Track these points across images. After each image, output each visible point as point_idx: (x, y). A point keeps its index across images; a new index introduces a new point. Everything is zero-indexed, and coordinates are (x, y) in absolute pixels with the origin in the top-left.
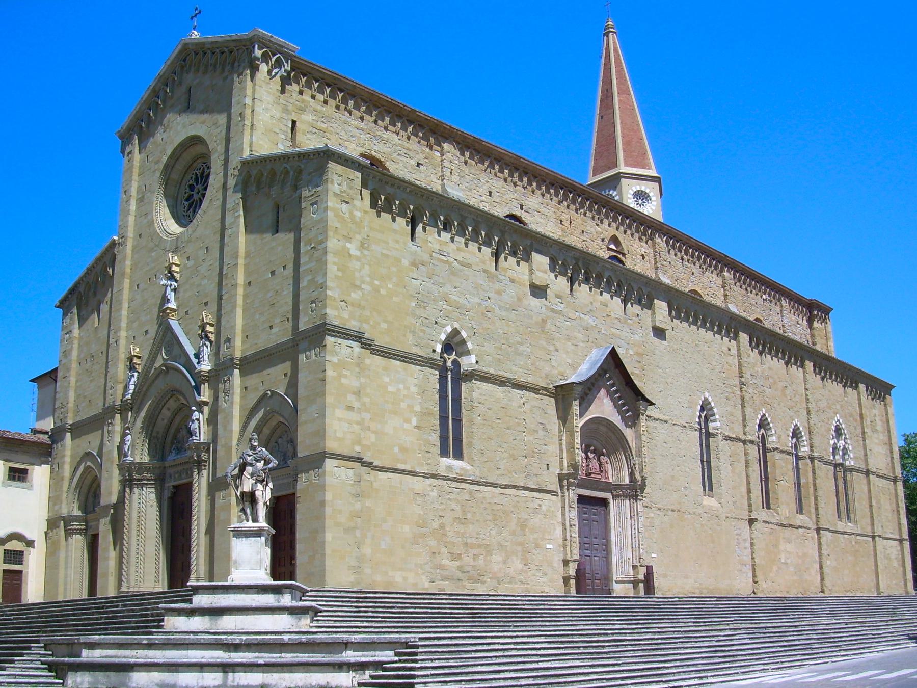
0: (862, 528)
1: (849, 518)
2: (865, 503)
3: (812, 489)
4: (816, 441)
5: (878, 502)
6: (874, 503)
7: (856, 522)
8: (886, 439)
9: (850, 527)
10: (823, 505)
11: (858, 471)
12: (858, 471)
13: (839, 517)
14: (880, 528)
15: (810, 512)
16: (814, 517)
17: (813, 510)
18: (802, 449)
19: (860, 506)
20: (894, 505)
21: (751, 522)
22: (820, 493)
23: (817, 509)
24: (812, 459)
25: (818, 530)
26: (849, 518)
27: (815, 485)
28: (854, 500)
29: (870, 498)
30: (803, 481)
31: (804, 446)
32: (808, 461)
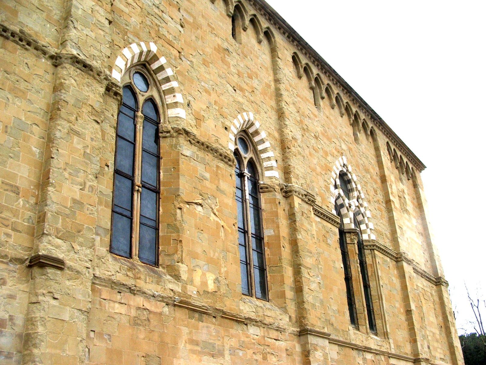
0: (398, 347)
1: (372, 326)
2: (398, 305)
3: (286, 252)
4: (296, 164)
5: (420, 307)
6: (413, 307)
7: (386, 335)
8: (420, 228)
9: (374, 342)
10: (314, 286)
11: (384, 252)
12: (384, 252)
13: (354, 320)
14: (426, 349)
15: (282, 295)
16: (292, 307)
17: (290, 294)
18: (267, 174)
19: (390, 307)
20: (440, 318)
21: (38, 263)
22: (307, 261)
23: (299, 289)
24: (287, 193)
25: (303, 332)
26: (372, 326)
27: (294, 244)
28: (380, 298)
29: (406, 298)
30: (268, 233)
31: (271, 168)
32: (279, 196)
